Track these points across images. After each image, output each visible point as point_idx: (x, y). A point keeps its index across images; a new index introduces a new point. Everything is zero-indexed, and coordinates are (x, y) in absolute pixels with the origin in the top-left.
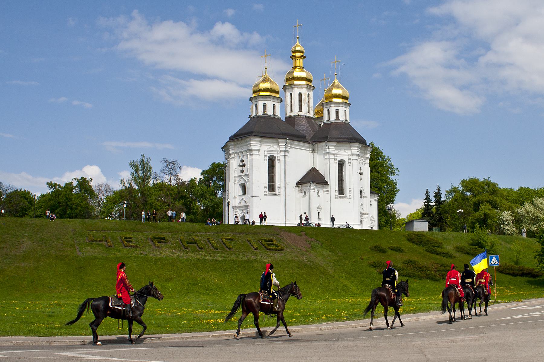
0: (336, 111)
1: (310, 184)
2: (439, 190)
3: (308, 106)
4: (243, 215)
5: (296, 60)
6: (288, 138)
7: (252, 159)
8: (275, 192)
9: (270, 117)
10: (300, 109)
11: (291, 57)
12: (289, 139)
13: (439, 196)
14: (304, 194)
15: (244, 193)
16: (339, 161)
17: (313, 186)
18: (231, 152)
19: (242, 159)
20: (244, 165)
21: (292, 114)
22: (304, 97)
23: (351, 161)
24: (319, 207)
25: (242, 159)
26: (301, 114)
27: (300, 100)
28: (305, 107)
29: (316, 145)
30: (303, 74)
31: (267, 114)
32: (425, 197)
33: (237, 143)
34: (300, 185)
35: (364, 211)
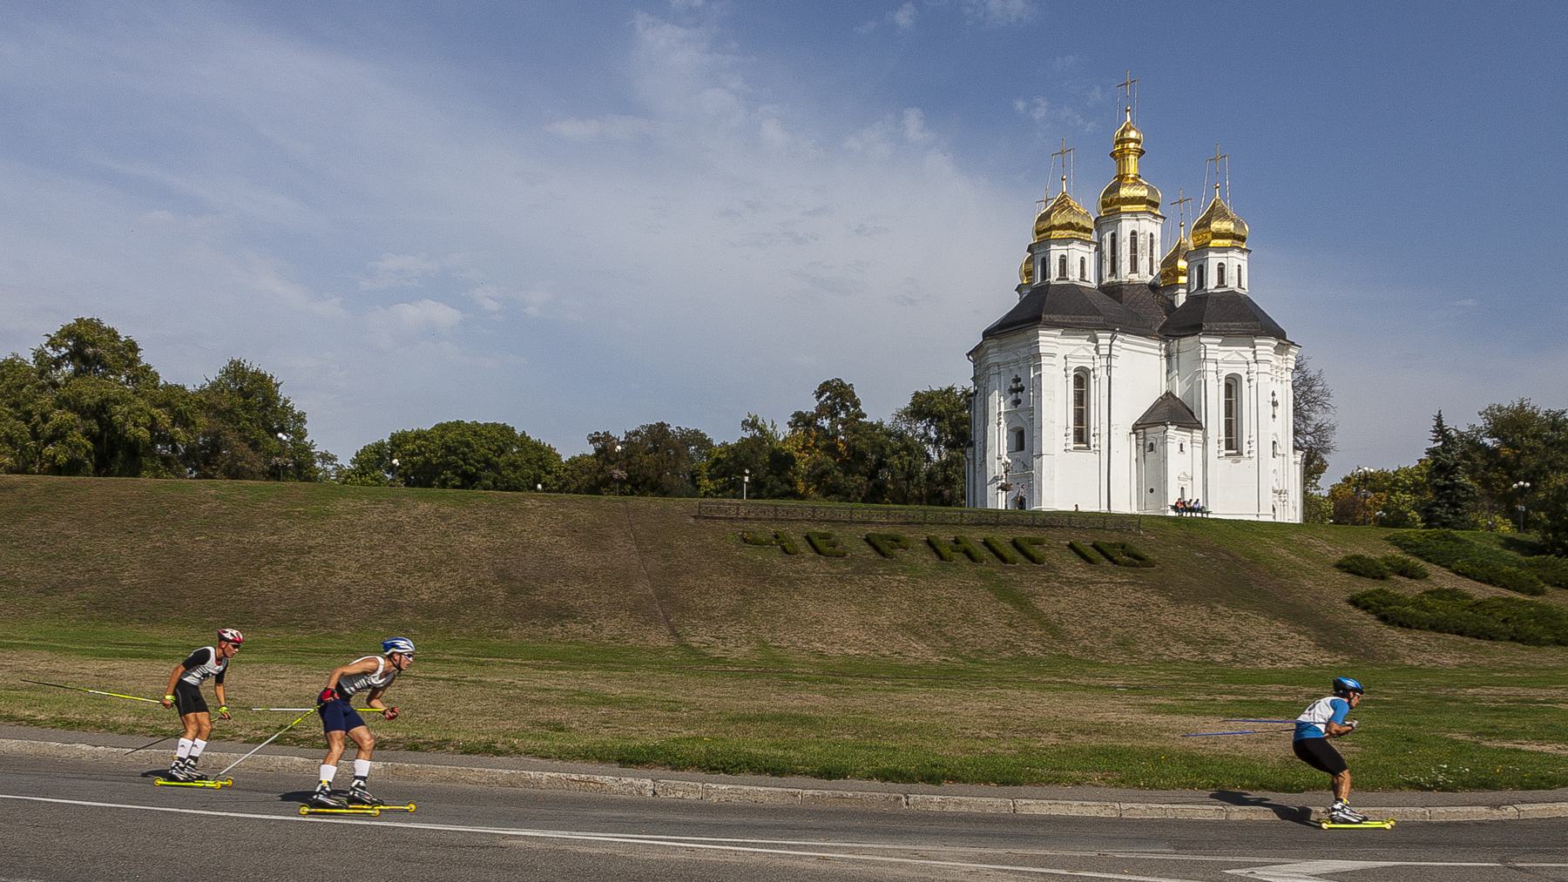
0: (1219, 268)
1: (1166, 426)
3: (1151, 260)
6: (1118, 329)
7: (1040, 375)
9: (1073, 286)
10: (1134, 269)
11: (1112, 155)
12: (1120, 331)
14: (1147, 449)
16: (1226, 378)
17: (1171, 430)
18: (990, 361)
19: (1016, 376)
20: (1021, 389)
21: (1113, 279)
22: (1141, 240)
23: (1254, 376)
24: (1182, 476)
25: (1016, 376)
26: (1134, 277)
27: (1134, 249)
28: (1143, 263)
29: (1176, 341)
30: (1142, 192)
31: (1068, 279)
33: (1004, 341)
34: (1142, 430)
35: (1279, 485)
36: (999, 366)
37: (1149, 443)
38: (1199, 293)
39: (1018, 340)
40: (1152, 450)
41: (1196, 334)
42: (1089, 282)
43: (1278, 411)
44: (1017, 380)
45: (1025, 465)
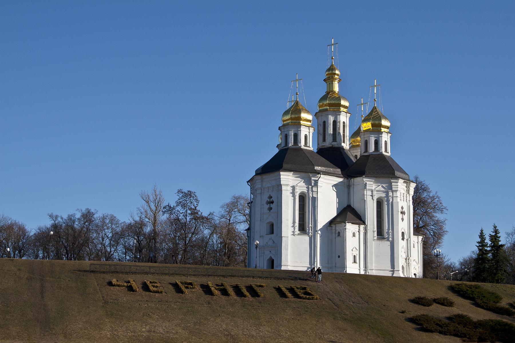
2: (496, 231)
4: (271, 257)
5: (330, 83)
8: (305, 232)
12: (322, 174)
13: (496, 239)
14: (337, 235)
15: (272, 232)
18: (257, 187)
20: (272, 202)
26: (334, 143)
29: (352, 179)
32: (479, 240)
34: (334, 225)
36: (261, 189)
37: (337, 232)
38: (366, 154)
39: (269, 178)
40: (339, 235)
41: (362, 176)
42: (309, 147)
43: (405, 217)
44: (270, 197)
45: (274, 242)
